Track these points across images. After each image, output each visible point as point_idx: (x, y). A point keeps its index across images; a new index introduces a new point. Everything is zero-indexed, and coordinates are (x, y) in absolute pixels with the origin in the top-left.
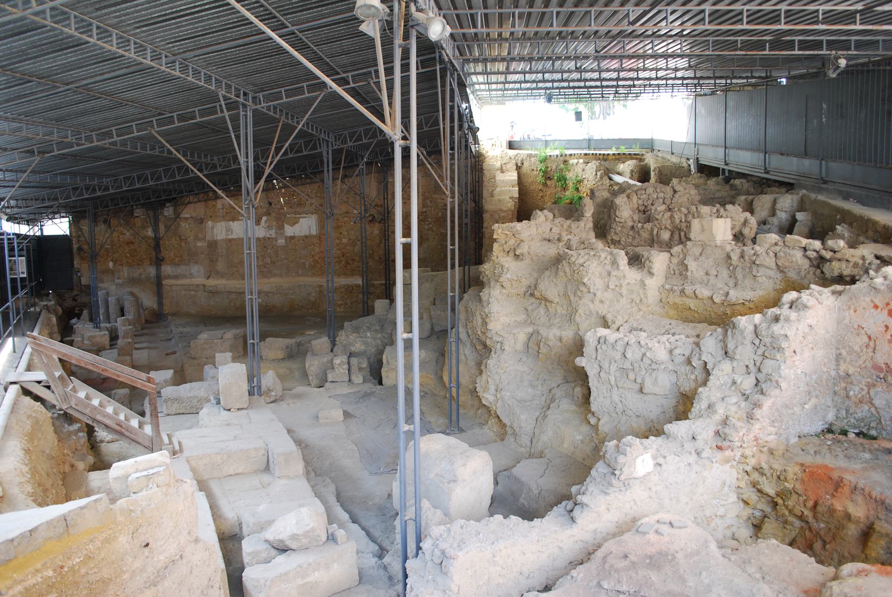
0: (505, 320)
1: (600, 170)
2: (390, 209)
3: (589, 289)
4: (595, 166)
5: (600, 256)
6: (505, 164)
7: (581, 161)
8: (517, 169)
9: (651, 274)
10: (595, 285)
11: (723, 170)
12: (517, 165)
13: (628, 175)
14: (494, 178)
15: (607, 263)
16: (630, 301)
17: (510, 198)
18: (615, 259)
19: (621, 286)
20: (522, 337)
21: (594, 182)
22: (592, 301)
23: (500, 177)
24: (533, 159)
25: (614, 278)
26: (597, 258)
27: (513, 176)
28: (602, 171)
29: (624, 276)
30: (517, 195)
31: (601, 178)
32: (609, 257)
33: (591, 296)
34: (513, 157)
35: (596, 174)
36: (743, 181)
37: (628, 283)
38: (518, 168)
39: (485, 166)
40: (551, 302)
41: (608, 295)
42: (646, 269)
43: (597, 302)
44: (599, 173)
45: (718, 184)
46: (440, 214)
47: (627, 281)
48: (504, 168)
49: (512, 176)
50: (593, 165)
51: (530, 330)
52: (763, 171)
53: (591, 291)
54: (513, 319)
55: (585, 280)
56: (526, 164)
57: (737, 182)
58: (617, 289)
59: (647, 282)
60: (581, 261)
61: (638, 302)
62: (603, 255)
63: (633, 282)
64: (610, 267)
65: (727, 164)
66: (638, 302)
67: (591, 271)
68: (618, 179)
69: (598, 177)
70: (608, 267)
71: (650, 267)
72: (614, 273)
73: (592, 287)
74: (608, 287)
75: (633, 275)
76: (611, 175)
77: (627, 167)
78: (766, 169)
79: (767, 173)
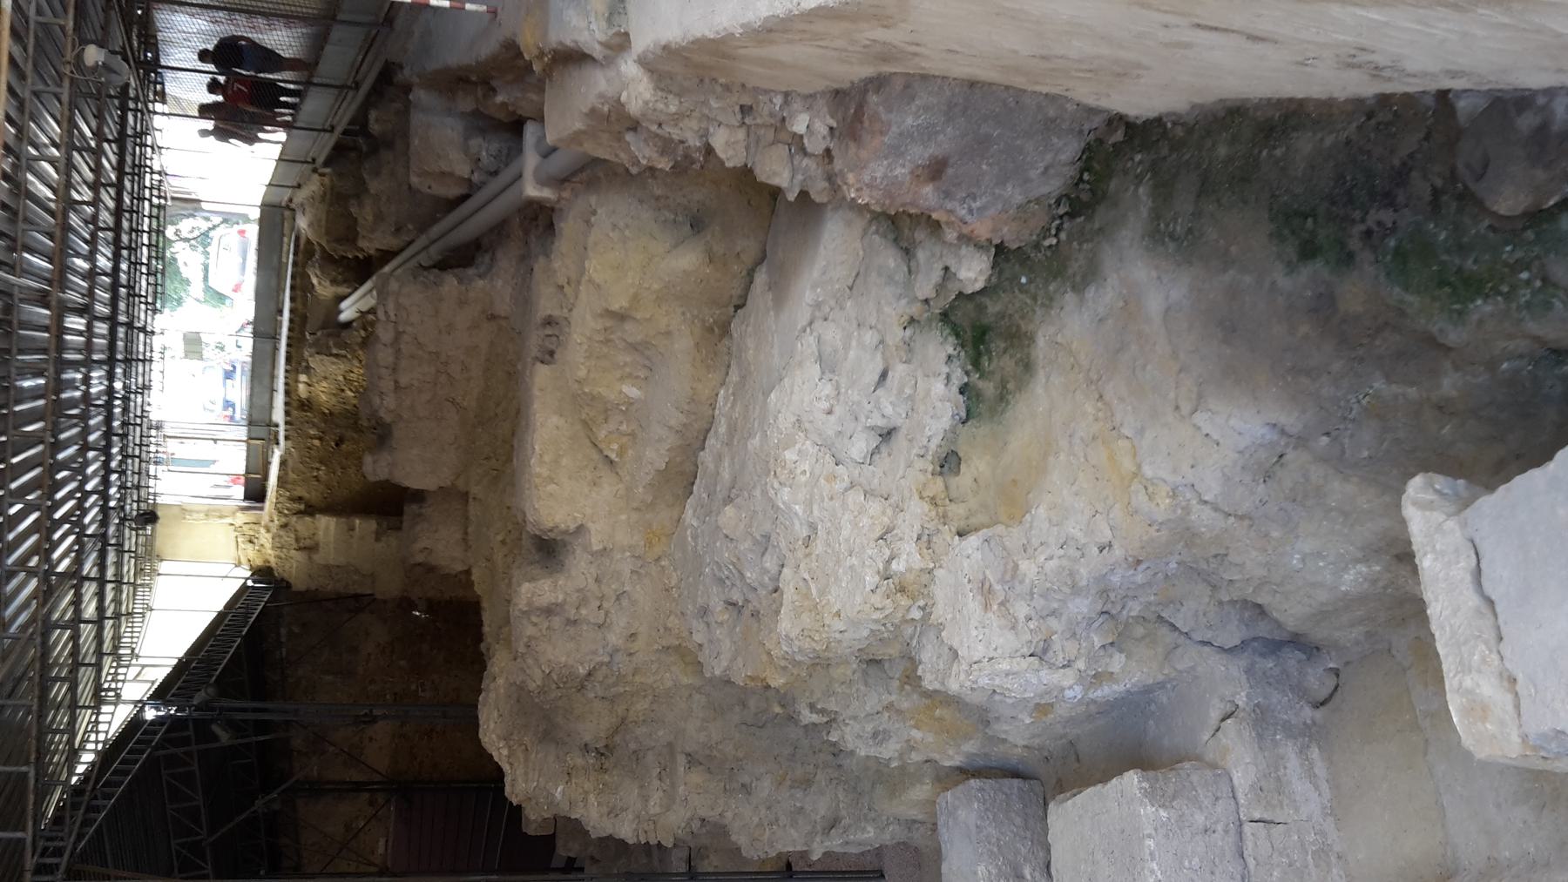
0: (654, 807)
1: (328, 348)
2: (378, 778)
3: (601, 664)
4: (318, 357)
5: (530, 638)
6: (297, 540)
7: (303, 378)
8: (312, 514)
9: (580, 529)
10: (595, 653)
11: (345, 133)
12: (299, 513)
13: (342, 290)
14: (327, 567)
15: (546, 625)
16: (635, 577)
17: (377, 539)
18: (538, 609)
19: (602, 598)
20: (696, 777)
21: (356, 363)
22: (631, 654)
23: (329, 554)
24: (292, 476)
25: (584, 612)
26: (533, 643)
27: (326, 526)
28: (331, 343)
29: (579, 591)
30: (372, 525)
31: (345, 346)
32: (534, 619)
33: (618, 658)
34: (284, 520)
35: (336, 356)
36: (373, 115)
37: (597, 580)
38: (310, 510)
39: (299, 584)
40: (623, 720)
41: (620, 622)
42: (567, 538)
43: (636, 646)
44: (335, 351)
45: (377, 173)
46: (402, 663)
47: (593, 586)
48: (308, 543)
49: (327, 528)
50: (316, 362)
51: (681, 760)
52: (351, 94)
53: (606, 659)
54: (656, 783)
55: (582, 671)
56: (300, 491)
57: (375, 128)
58: (605, 605)
59: (596, 547)
60: (537, 674)
61: (639, 563)
62: (530, 631)
63: (593, 570)
64: (557, 619)
65: (332, 129)
66: (639, 563)
67: (563, 659)
68: (348, 311)
69: (343, 352)
70: (557, 622)
71: (566, 532)
72: (572, 613)
73: (599, 659)
74: (599, 627)
75: (579, 570)
76: (343, 317)
77: (323, 288)
78: (350, 88)
79: (357, 86)
